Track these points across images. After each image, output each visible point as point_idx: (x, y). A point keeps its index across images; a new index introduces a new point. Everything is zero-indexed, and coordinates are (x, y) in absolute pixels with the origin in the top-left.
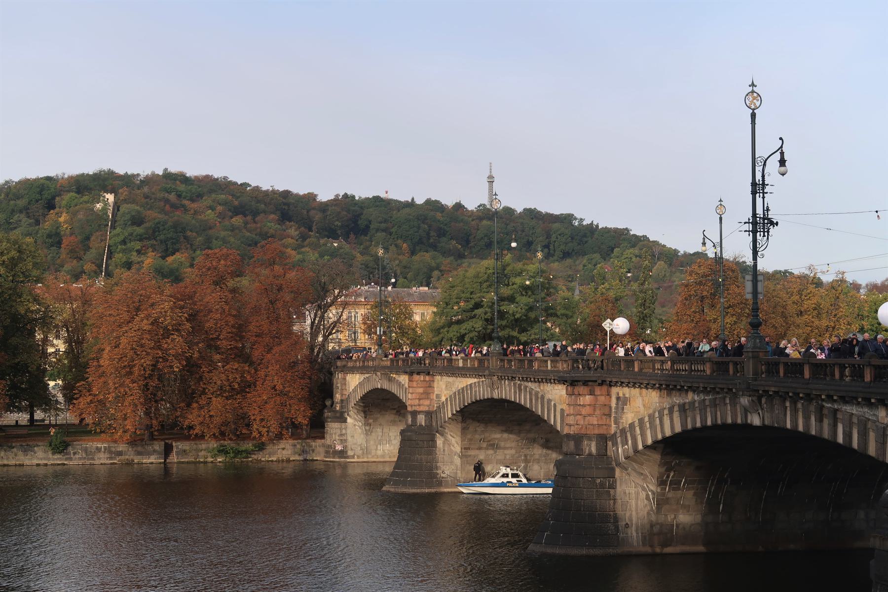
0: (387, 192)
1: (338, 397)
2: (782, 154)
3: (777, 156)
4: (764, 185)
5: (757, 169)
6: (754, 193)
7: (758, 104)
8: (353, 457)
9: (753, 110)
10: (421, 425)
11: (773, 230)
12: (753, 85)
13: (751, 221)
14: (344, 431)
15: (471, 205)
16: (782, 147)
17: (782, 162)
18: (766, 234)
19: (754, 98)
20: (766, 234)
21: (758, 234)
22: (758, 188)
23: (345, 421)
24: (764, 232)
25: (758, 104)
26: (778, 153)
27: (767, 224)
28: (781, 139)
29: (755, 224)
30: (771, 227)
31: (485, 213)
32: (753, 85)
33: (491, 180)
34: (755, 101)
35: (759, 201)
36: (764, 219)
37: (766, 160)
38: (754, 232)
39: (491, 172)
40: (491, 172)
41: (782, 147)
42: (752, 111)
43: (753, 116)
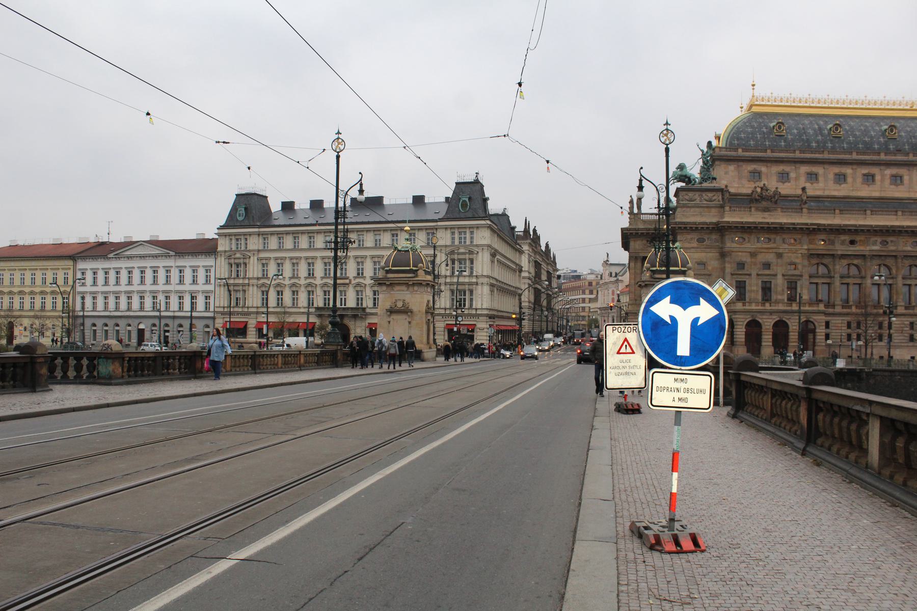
2: (361, 185)
5: (340, 199)
7: (342, 148)
9: (338, 152)
12: (339, 133)
13: (333, 240)
16: (361, 180)
18: (345, 250)
19: (339, 143)
20: (345, 250)
21: (339, 250)
24: (344, 249)
25: (342, 148)
26: (358, 185)
27: (347, 242)
28: (360, 173)
30: (350, 245)
32: (339, 133)
34: (340, 146)
37: (347, 192)
41: (361, 180)
42: (337, 154)
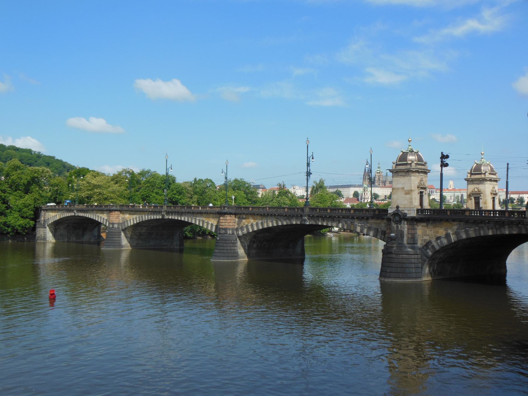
1: (42, 219)
3: (312, 157)
4: (309, 164)
6: (307, 166)
8: (49, 240)
10: (116, 228)
11: (311, 175)
12: (308, 138)
14: (45, 231)
17: (313, 158)
22: (308, 165)
23: (46, 228)
29: (307, 173)
35: (308, 168)
36: (309, 172)
38: (307, 176)
43: (308, 146)
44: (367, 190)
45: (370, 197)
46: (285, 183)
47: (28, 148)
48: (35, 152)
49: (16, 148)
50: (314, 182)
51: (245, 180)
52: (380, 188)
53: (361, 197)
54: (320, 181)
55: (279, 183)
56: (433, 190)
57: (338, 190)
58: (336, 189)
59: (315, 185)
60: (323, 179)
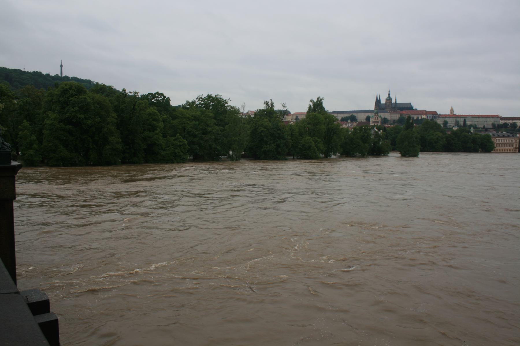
0: (24, 69)
15: (52, 74)
31: (57, 77)
33: (61, 66)
39: (61, 63)
40: (61, 63)
44: (377, 115)
45: (380, 121)
46: (273, 102)
47: (88, 79)
48: (93, 82)
49: (78, 79)
50: (311, 101)
51: (221, 97)
52: (389, 114)
53: (372, 121)
54: (318, 98)
55: (266, 101)
56: (436, 115)
57: (352, 115)
58: (351, 114)
59: (312, 105)
60: (321, 97)
